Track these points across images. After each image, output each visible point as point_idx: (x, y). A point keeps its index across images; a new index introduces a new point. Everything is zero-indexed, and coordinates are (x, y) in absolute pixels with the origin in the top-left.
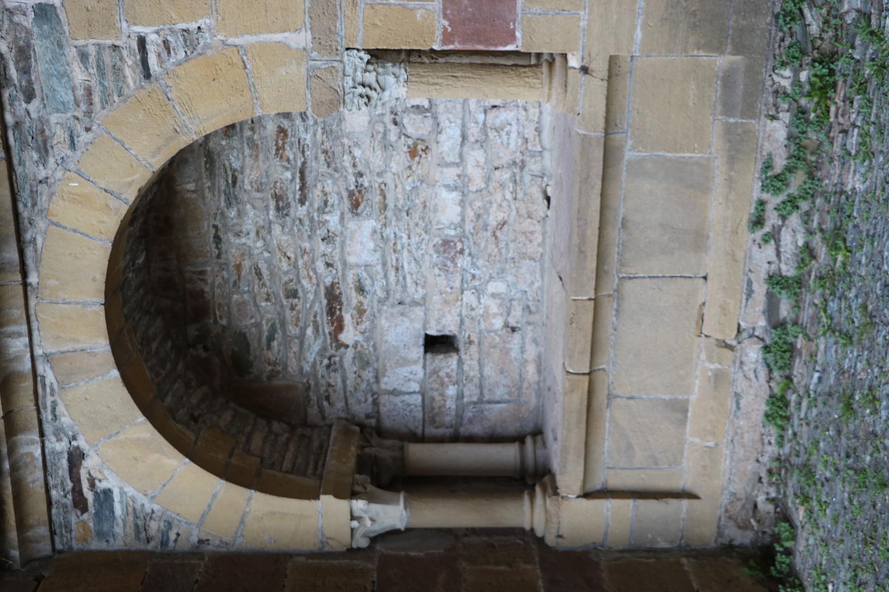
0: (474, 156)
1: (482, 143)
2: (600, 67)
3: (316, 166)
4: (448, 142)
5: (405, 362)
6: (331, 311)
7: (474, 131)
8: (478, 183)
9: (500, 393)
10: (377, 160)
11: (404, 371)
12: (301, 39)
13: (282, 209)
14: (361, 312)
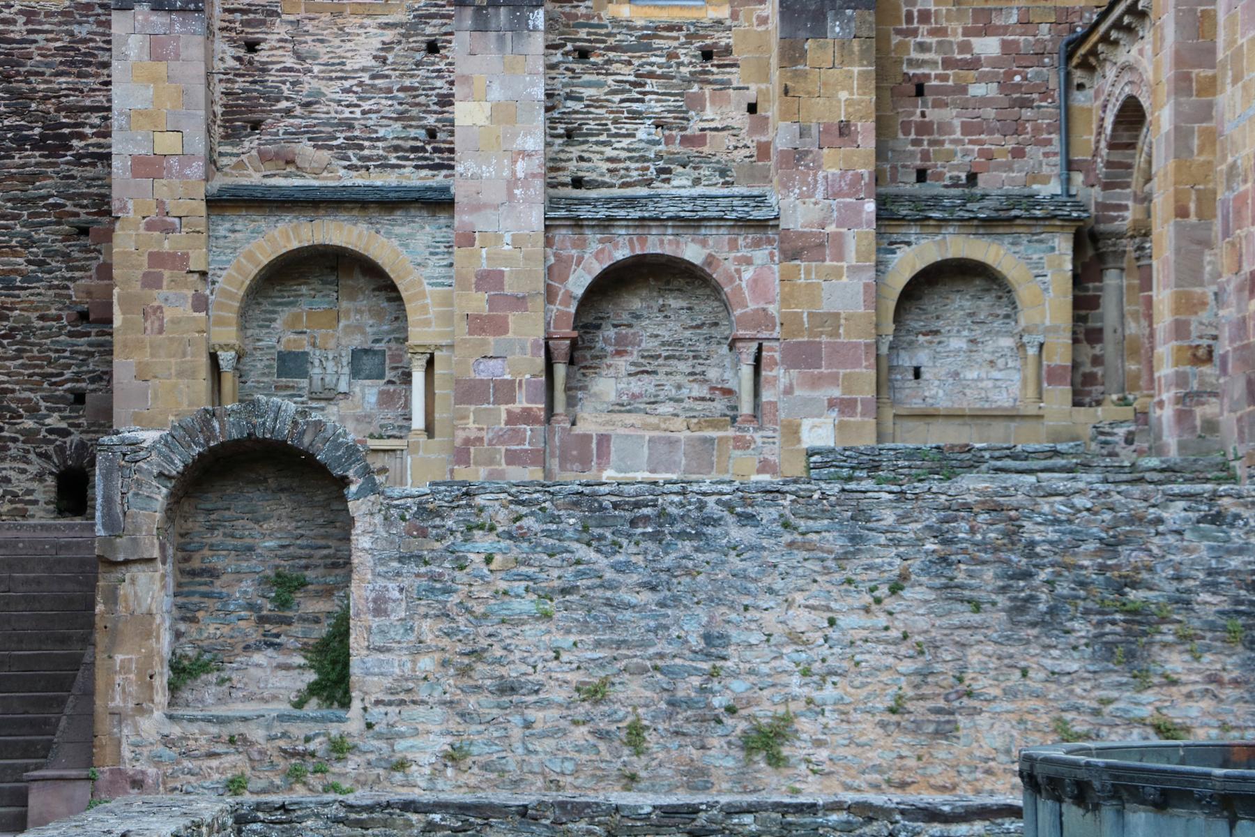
0: (990, 384)
1: (995, 387)
2: (1041, 412)
3: (985, 328)
4: (996, 374)
5: (911, 359)
6: (931, 332)
7: (999, 383)
8: (980, 385)
9: (898, 395)
10: (989, 349)
11: (907, 358)
12: (1048, 323)
13: (971, 315)
14: (931, 342)
